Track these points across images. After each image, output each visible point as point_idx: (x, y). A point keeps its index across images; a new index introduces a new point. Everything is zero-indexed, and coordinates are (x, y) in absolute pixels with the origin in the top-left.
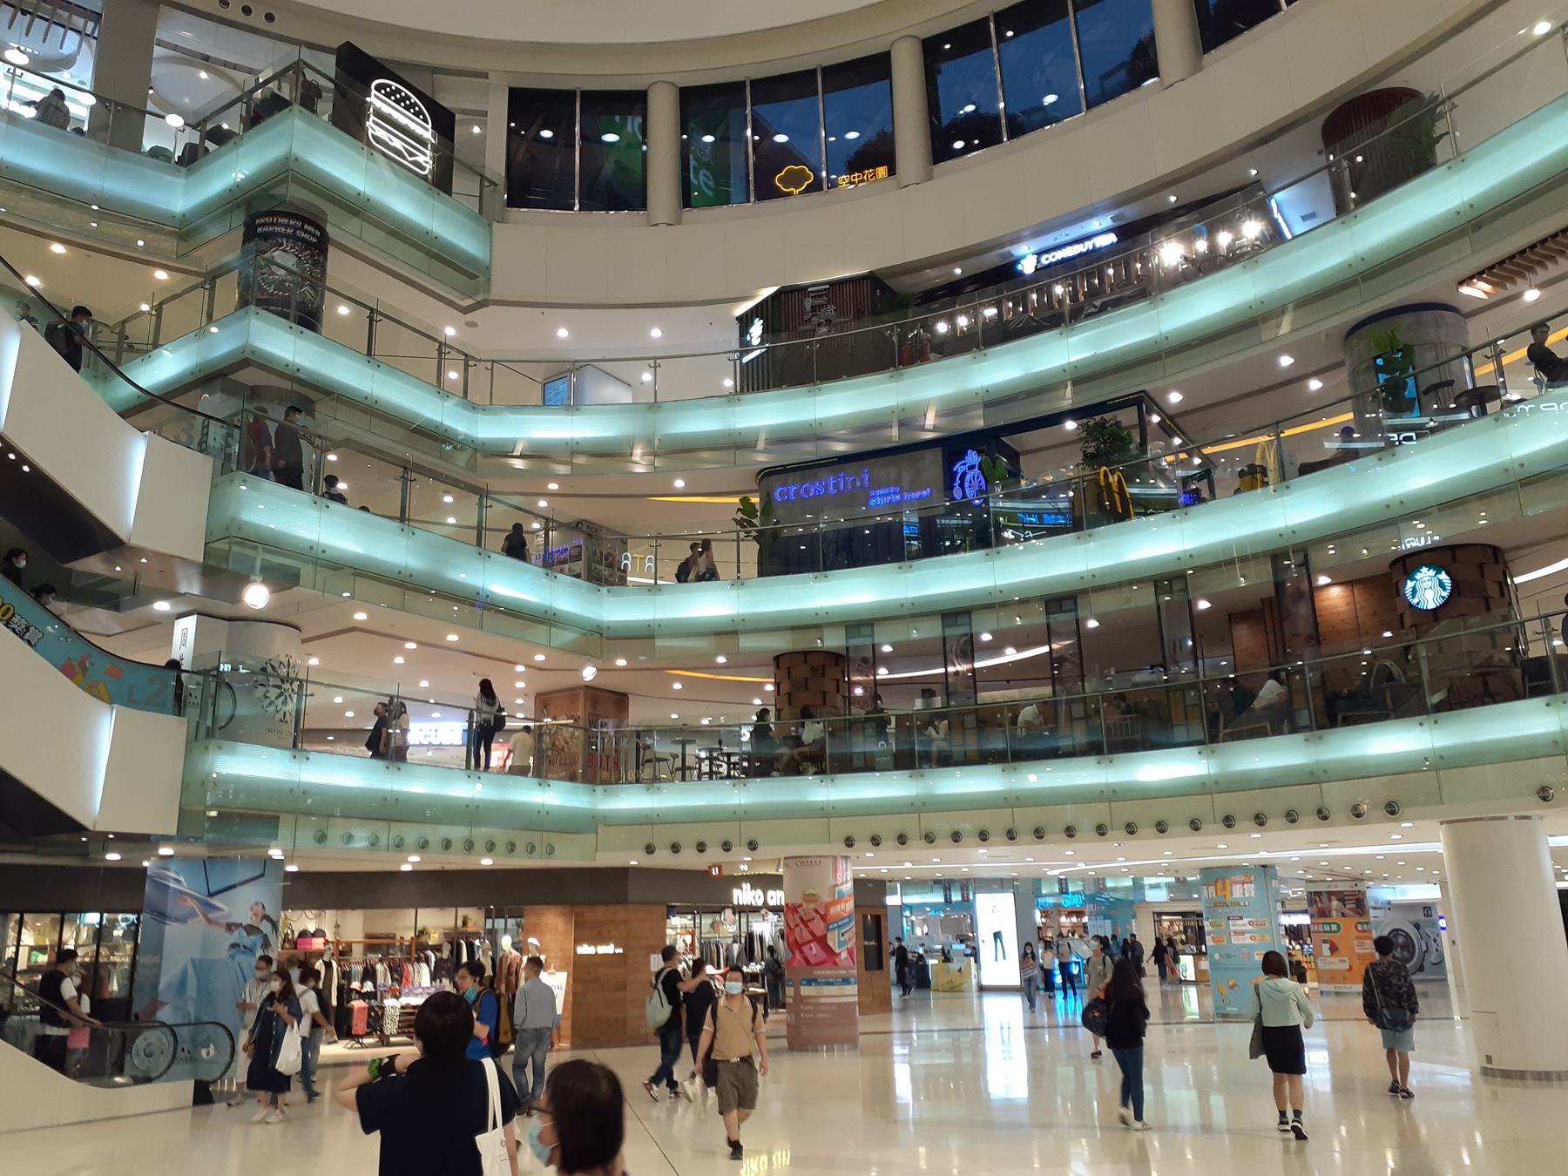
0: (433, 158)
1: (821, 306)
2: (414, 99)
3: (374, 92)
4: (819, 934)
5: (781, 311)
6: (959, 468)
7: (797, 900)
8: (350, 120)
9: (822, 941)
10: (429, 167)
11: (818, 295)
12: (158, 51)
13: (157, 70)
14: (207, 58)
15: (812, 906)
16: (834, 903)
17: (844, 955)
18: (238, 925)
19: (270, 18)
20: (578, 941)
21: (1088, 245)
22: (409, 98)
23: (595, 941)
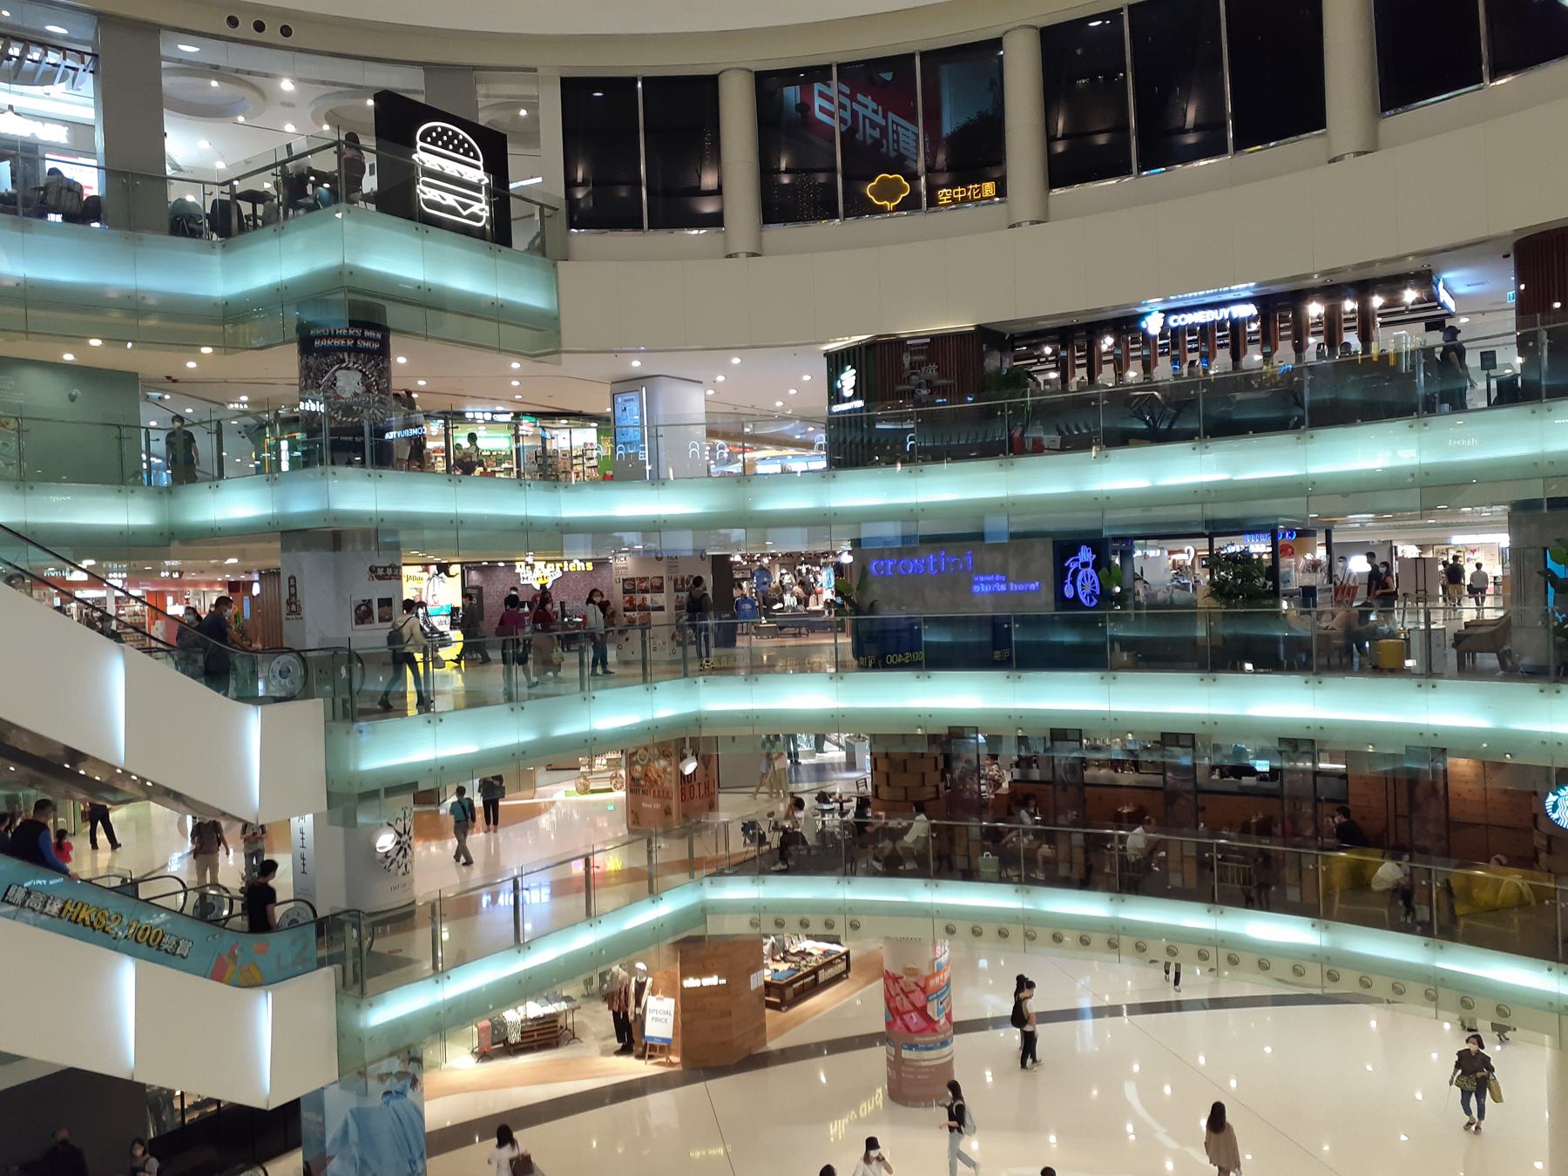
0: (489, 203)
1: (921, 364)
2: (463, 134)
3: (420, 144)
4: (919, 1005)
5: (880, 363)
6: (1072, 565)
7: (898, 972)
8: (398, 201)
9: (922, 1011)
10: (485, 215)
11: (916, 350)
12: (164, 64)
13: (167, 81)
14: (217, 67)
15: (913, 979)
16: (934, 975)
17: (943, 1021)
18: (389, 1075)
19: (286, 31)
20: (684, 975)
21: (1224, 313)
22: (456, 135)
23: (699, 974)
